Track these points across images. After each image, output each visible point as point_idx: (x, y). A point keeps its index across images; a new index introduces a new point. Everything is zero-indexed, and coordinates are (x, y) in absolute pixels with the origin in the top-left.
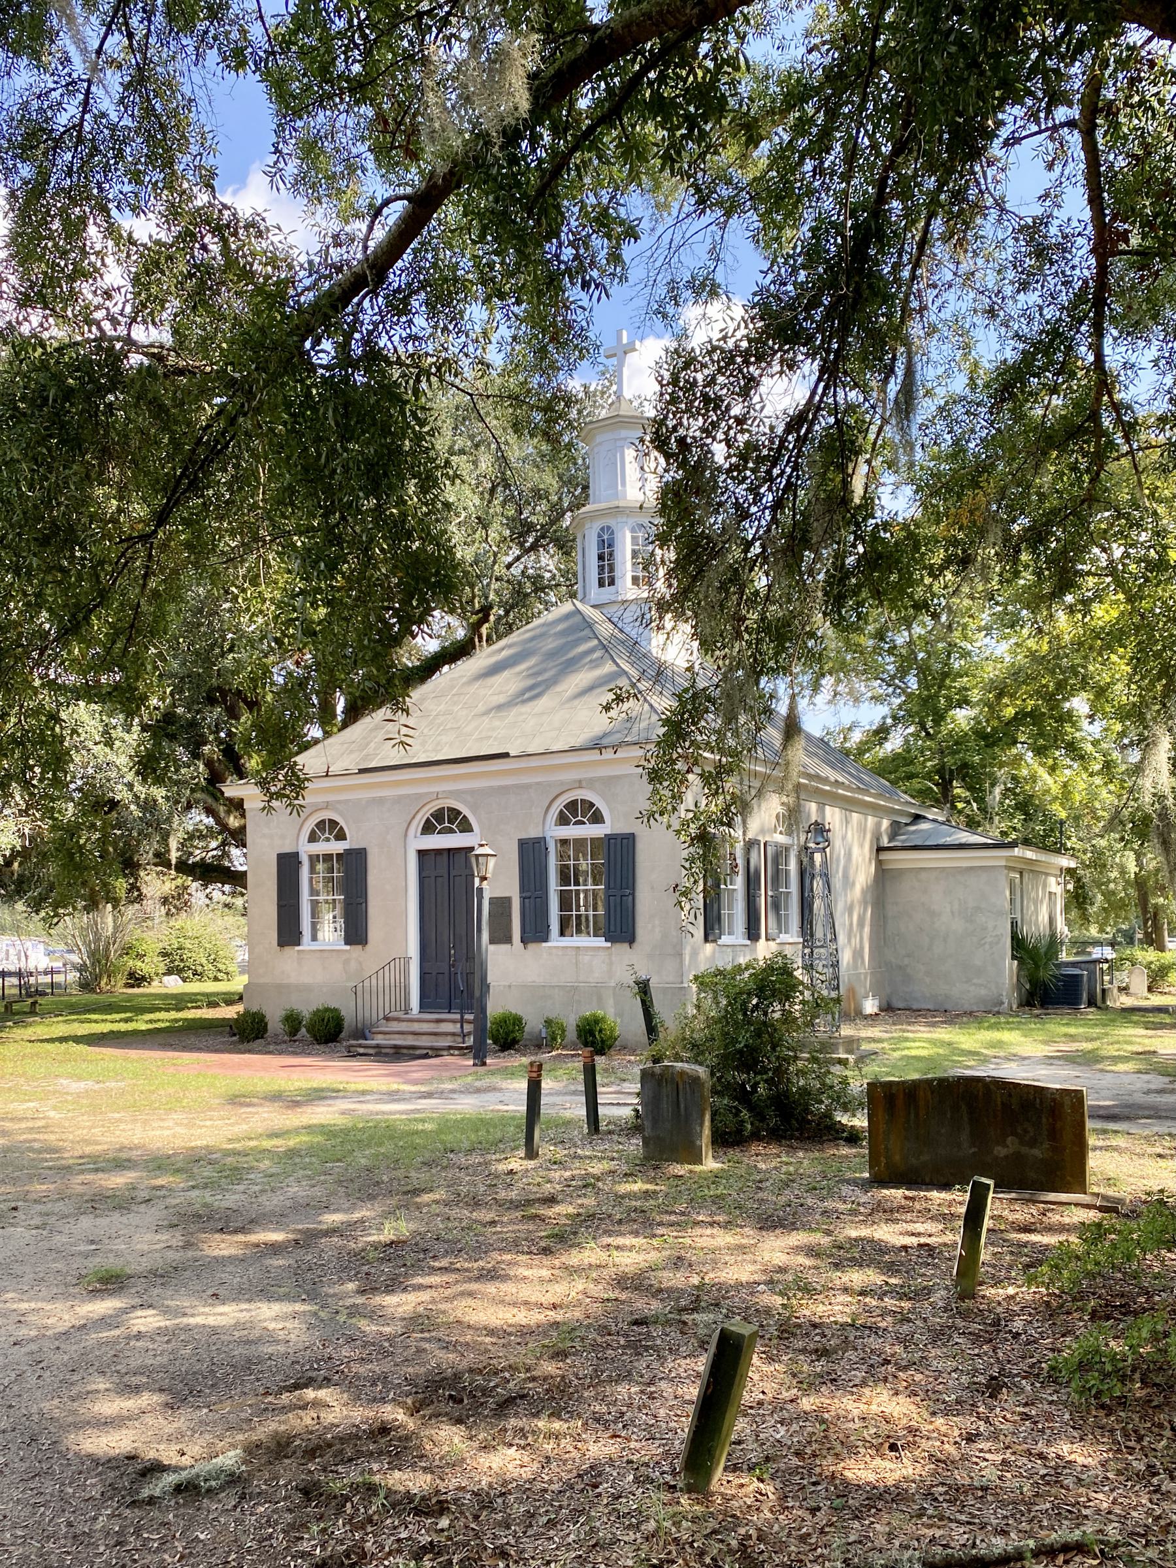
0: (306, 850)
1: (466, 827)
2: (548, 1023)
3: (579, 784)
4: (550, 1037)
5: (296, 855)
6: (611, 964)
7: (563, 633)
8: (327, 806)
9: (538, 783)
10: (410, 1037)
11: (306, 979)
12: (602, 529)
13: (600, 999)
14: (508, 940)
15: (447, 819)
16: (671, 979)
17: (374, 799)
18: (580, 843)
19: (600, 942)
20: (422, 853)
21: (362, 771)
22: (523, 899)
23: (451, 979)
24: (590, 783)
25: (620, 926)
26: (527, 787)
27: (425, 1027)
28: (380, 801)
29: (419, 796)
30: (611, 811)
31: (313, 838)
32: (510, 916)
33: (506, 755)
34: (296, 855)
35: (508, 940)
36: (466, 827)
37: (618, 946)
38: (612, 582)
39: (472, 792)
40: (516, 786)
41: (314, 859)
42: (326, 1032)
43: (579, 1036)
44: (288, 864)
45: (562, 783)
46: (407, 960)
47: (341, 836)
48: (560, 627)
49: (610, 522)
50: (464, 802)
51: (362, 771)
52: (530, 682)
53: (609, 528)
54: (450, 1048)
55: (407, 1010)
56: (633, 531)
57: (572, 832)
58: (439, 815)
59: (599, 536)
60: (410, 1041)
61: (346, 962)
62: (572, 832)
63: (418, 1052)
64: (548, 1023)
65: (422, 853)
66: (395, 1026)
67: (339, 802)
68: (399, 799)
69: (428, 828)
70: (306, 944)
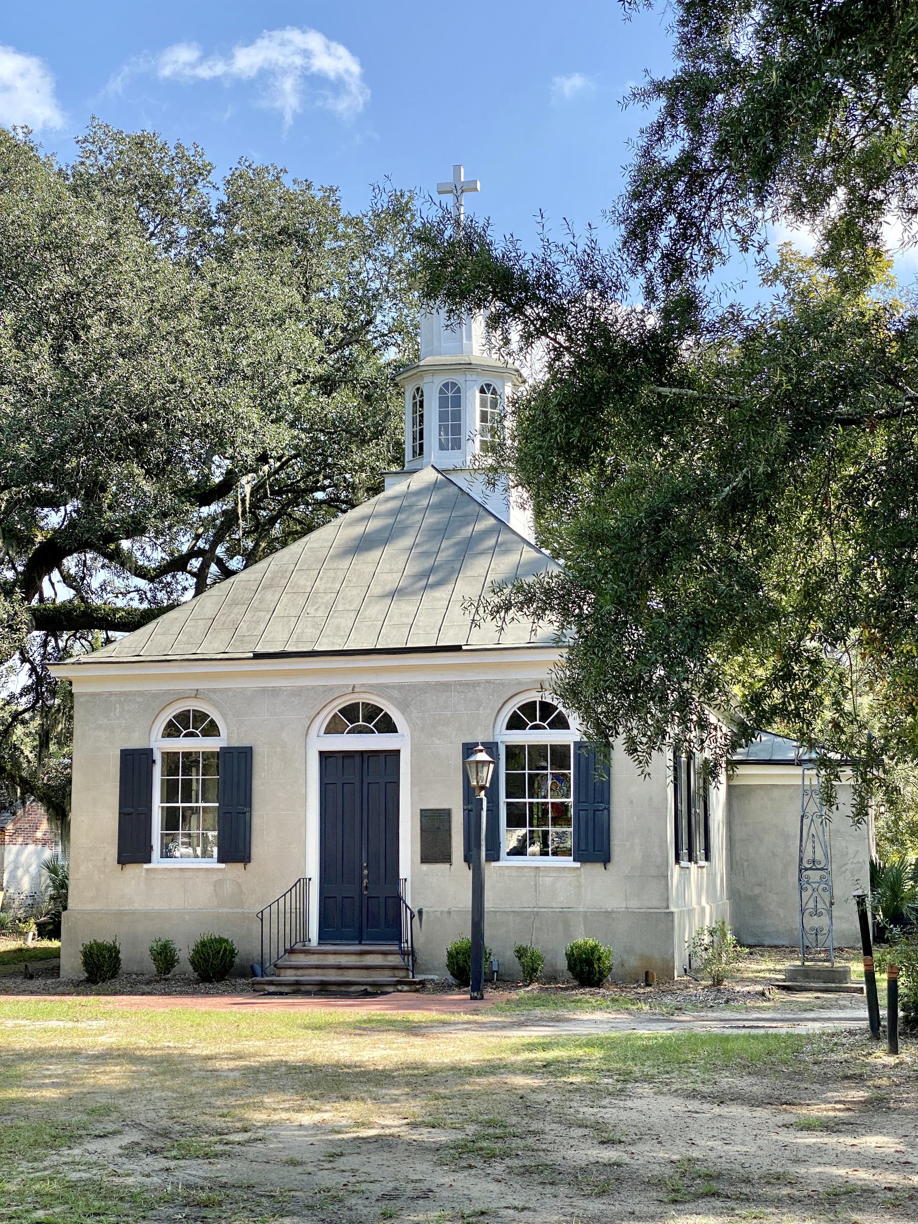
1: (387, 726)
2: (521, 953)
4: (530, 969)
5: (147, 754)
6: (580, 886)
7: (438, 507)
8: (197, 695)
9: (488, 682)
10: (333, 972)
11: (157, 905)
12: (446, 385)
13: (567, 925)
14: (446, 858)
15: (364, 716)
16: (654, 903)
17: (264, 690)
18: (538, 751)
19: (567, 862)
21: (258, 656)
23: (360, 904)
25: (594, 847)
26: (474, 685)
27: (331, 960)
28: (275, 692)
29: (331, 689)
32: (449, 830)
33: (458, 648)
34: (147, 754)
35: (446, 858)
36: (387, 726)
37: (589, 866)
38: (457, 445)
39: (400, 687)
40: (461, 684)
41: (170, 759)
42: (217, 968)
43: (571, 968)
44: (135, 764)
45: (519, 683)
46: (304, 882)
47: (212, 730)
48: (435, 498)
49: (458, 379)
50: (390, 699)
51: (258, 656)
52: (428, 564)
53: (454, 384)
54: (399, 983)
55: (306, 939)
56: (482, 391)
58: (350, 712)
59: (441, 392)
60: (332, 976)
61: (218, 884)
63: (353, 989)
64: (521, 953)
66: (301, 960)
67: (214, 691)
68: (299, 692)
69: (333, 728)
70: (157, 861)
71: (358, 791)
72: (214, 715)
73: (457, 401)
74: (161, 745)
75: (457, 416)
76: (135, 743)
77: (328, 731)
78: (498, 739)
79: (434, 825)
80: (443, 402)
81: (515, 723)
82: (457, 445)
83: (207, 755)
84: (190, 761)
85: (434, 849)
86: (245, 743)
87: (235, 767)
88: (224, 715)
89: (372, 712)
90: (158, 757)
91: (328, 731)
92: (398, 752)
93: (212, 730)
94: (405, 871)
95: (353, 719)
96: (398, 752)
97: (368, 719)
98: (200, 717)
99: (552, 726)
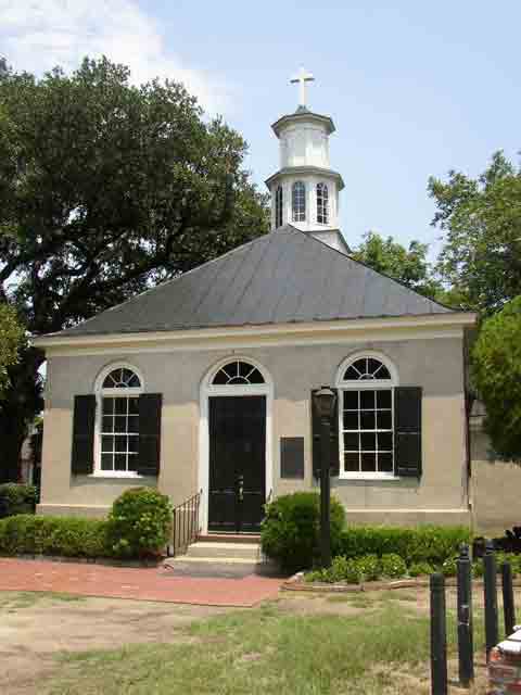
0: (101, 392)
3: (370, 346)
5: (91, 398)
15: (238, 371)
18: (367, 396)
20: (213, 401)
22: (315, 440)
24: (379, 346)
26: (317, 348)
28: (180, 354)
30: (398, 367)
31: (108, 384)
36: (257, 378)
38: (303, 218)
39: (267, 350)
41: (107, 401)
47: (134, 382)
57: (353, 385)
58: (231, 368)
62: (353, 385)
65: (213, 401)
68: (194, 355)
69: (220, 379)
71: (237, 428)
72: (137, 372)
73: (303, 192)
74: (101, 392)
75: (303, 201)
76: (85, 392)
77: (215, 382)
78: (338, 386)
79: (291, 448)
80: (295, 193)
81: (350, 375)
82: (303, 218)
83: (132, 400)
84: (121, 401)
85: (291, 467)
86: (157, 391)
87: (147, 411)
88: (143, 372)
89: (246, 368)
90: (99, 401)
91: (215, 382)
92: (264, 397)
93: (134, 382)
94: (269, 486)
95: (233, 373)
96: (264, 397)
97: (243, 373)
98: (129, 373)
99: (377, 377)
